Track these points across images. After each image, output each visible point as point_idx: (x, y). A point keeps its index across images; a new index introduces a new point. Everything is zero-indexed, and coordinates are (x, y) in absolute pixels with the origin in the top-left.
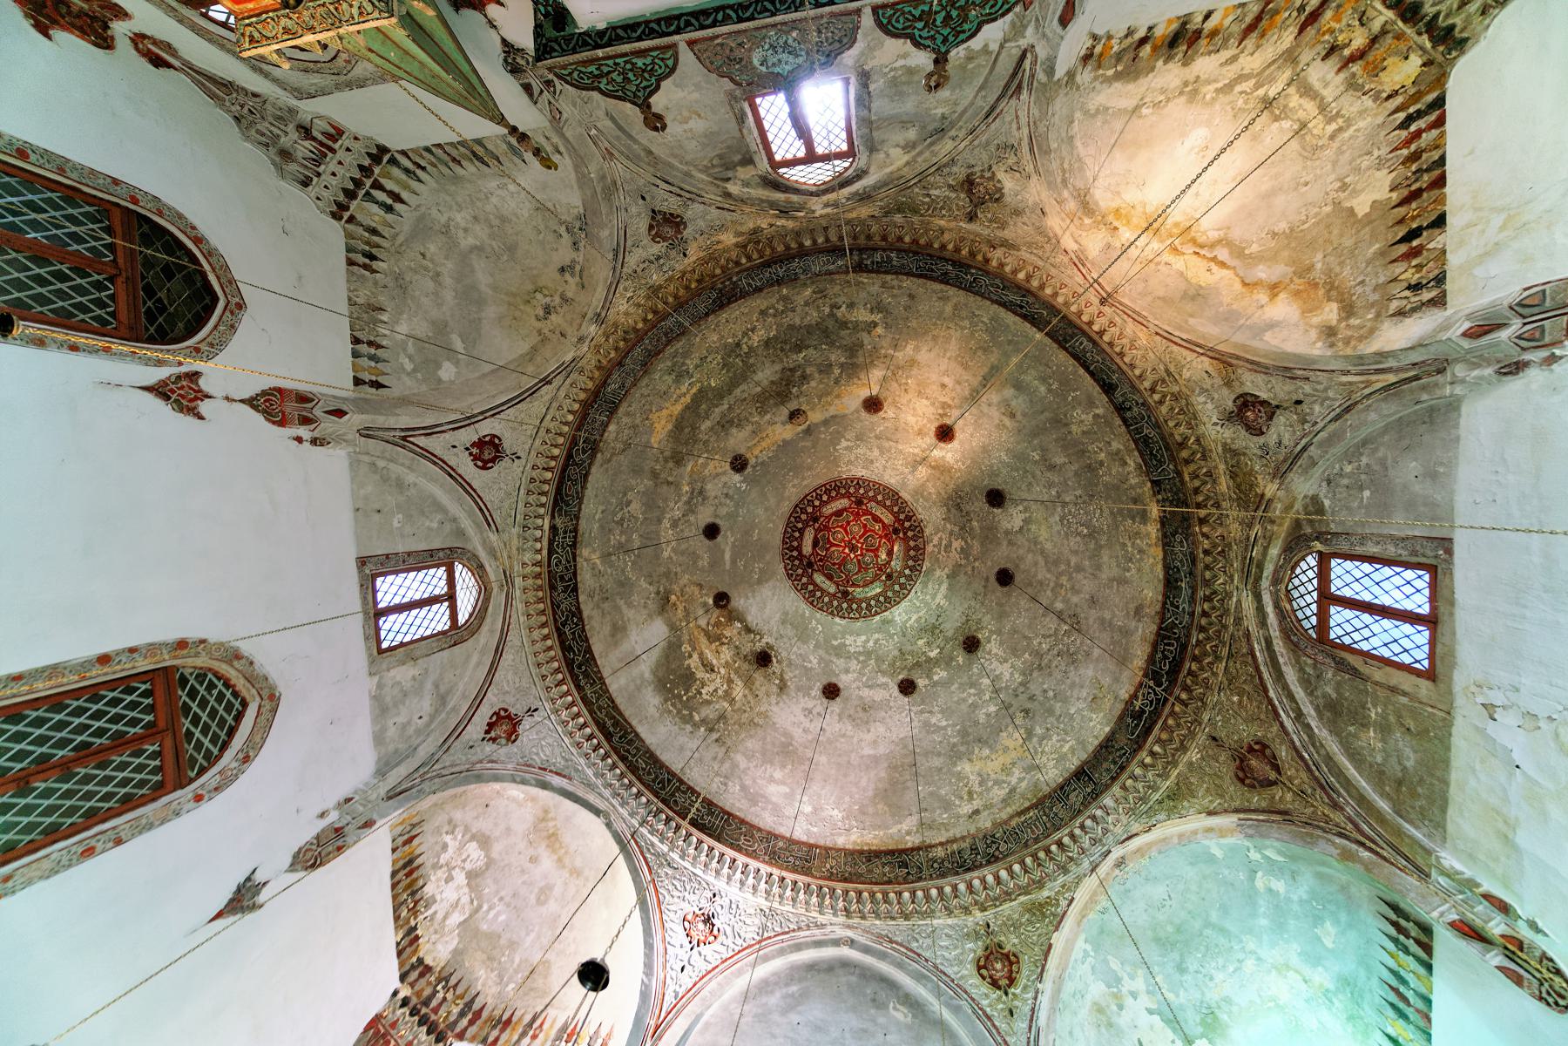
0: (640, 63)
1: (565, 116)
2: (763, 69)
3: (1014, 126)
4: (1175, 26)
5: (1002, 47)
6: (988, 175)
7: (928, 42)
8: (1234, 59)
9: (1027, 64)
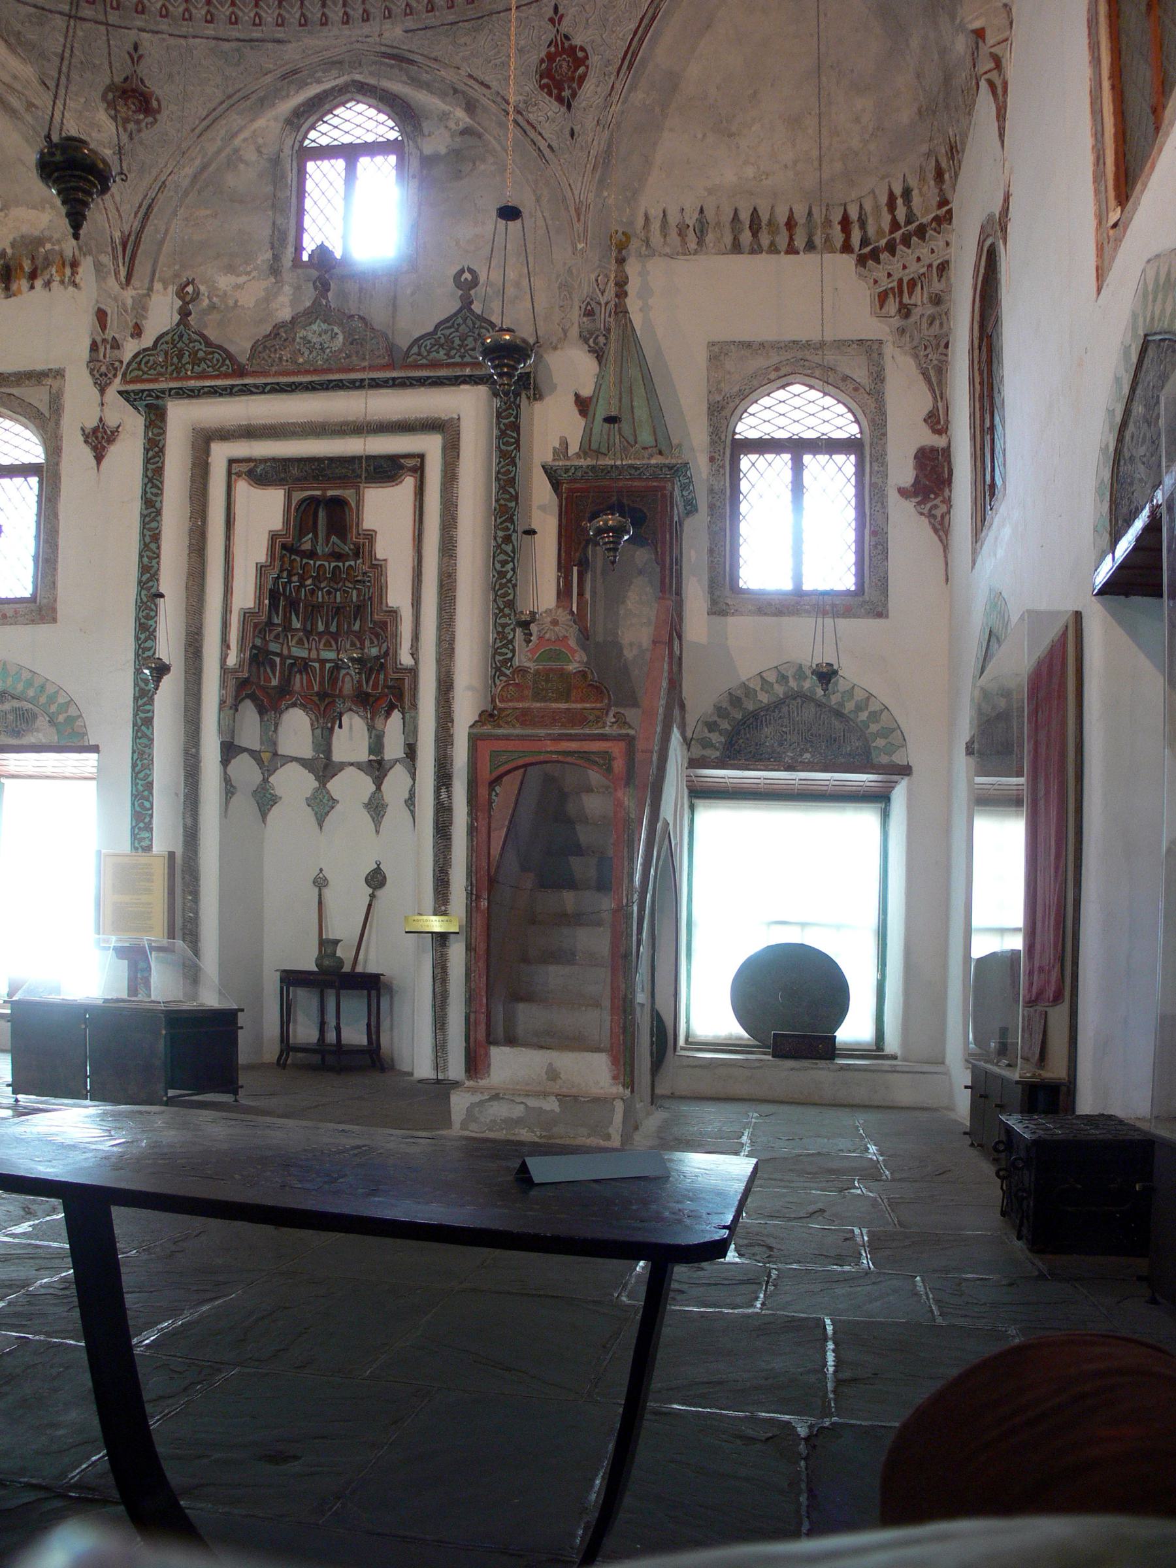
1: (593, 277)
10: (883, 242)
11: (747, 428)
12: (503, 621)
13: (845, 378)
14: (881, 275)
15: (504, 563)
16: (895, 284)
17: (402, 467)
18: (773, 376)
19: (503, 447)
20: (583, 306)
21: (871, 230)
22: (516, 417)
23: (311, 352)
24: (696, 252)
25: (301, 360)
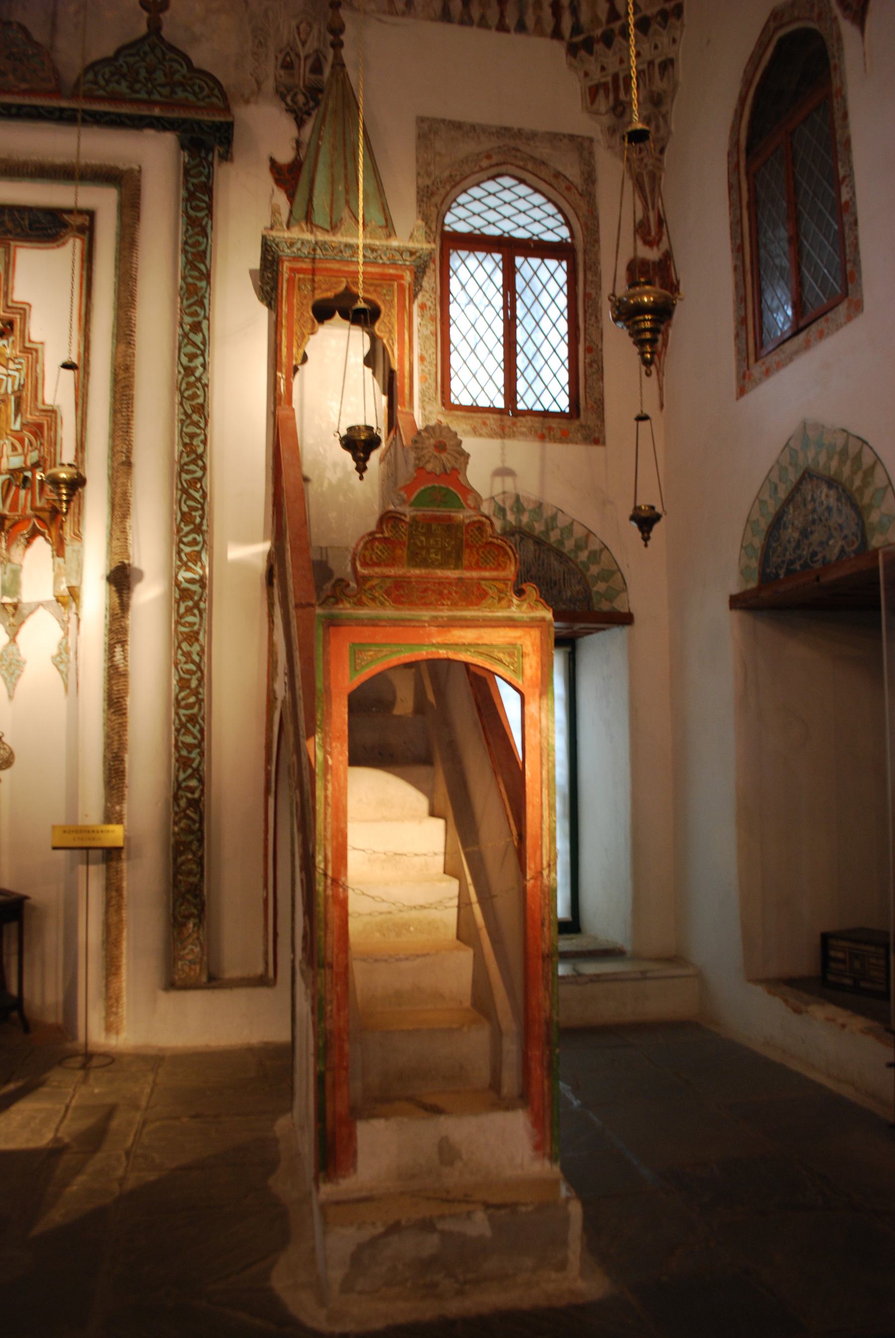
0: (123, 87)
1: (294, 23)
10: (599, 32)
11: (459, 220)
12: (192, 429)
13: (558, 175)
14: (593, 67)
15: (192, 357)
16: (609, 79)
17: (65, 225)
18: (485, 163)
19: (191, 212)
20: (281, 57)
21: (585, 17)
22: (210, 176)
24: (403, 14)
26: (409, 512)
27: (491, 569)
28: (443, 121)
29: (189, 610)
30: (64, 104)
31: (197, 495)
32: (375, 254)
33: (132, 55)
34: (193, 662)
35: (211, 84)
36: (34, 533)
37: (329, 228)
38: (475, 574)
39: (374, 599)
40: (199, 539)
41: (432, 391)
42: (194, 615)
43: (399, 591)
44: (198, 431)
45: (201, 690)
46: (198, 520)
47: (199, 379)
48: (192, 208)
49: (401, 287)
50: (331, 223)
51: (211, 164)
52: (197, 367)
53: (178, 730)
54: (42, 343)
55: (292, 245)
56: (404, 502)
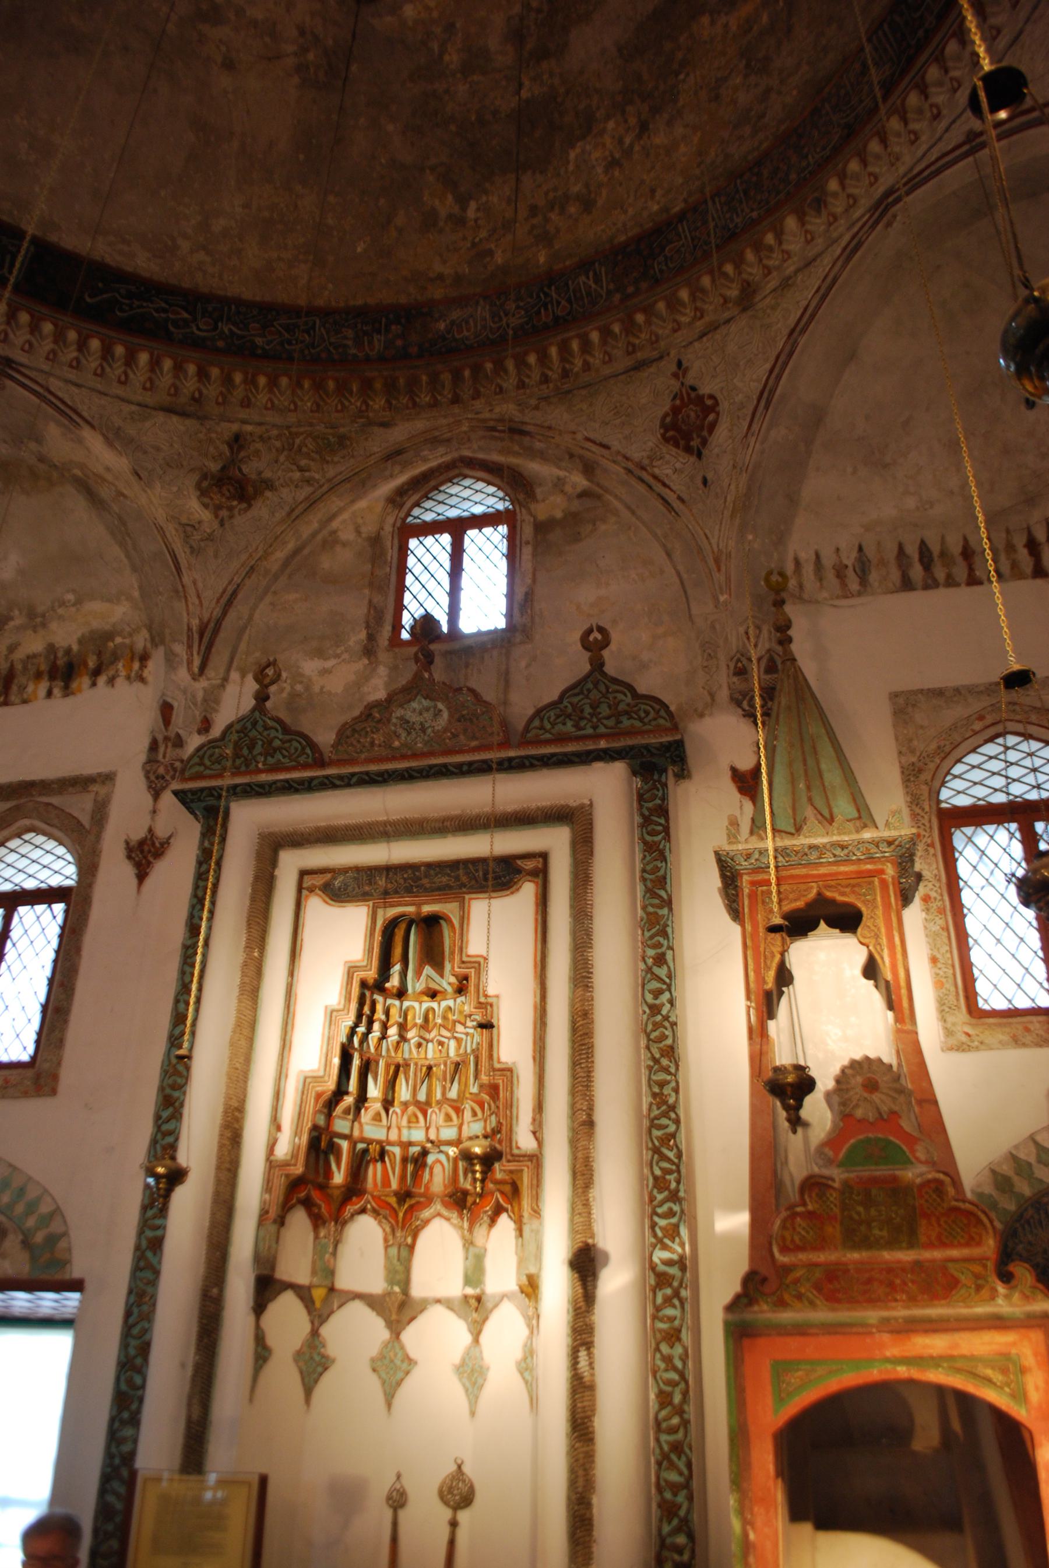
0: (569, 727)
1: (742, 630)
2: (440, 706)
3: (200, 585)
4: (74, 685)
5: (226, 679)
6: (224, 513)
7: (270, 723)
8: (12, 649)
9: (197, 662)
11: (957, 793)
12: (662, 1076)
15: (657, 993)
17: (519, 871)
18: (977, 726)
19: (648, 838)
20: (732, 665)
22: (664, 799)
23: (409, 733)
24: (859, 594)
25: (397, 744)
26: (838, 1175)
27: (960, 1245)
28: (921, 691)
29: (668, 1301)
30: (512, 753)
31: (671, 1155)
32: (846, 851)
33: (577, 694)
34: (675, 1369)
35: (657, 707)
36: (498, 1210)
37: (793, 831)
38: (937, 1254)
39: (799, 1297)
40: (676, 1208)
41: (952, 998)
42: (674, 1306)
43: (834, 1285)
44: (669, 1078)
45: (686, 1407)
46: (673, 1185)
47: (666, 1018)
48: (648, 833)
49: (884, 883)
50: (795, 825)
51: (665, 785)
52: (663, 1005)
53: (659, 1464)
54: (497, 996)
55: (748, 856)
56: (830, 1162)
